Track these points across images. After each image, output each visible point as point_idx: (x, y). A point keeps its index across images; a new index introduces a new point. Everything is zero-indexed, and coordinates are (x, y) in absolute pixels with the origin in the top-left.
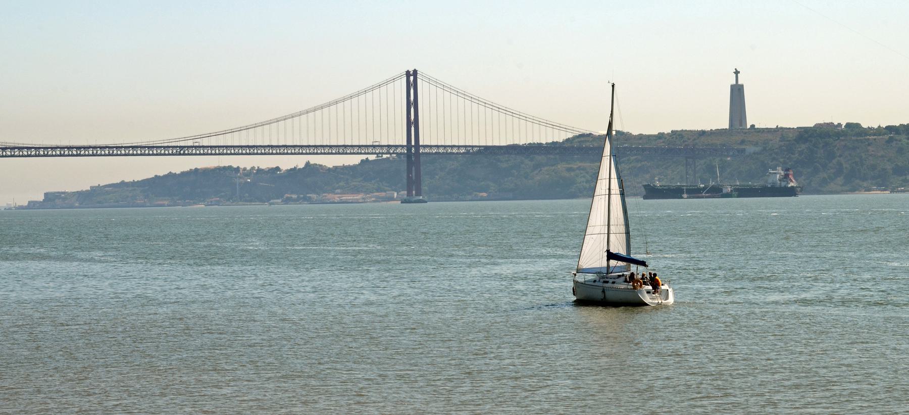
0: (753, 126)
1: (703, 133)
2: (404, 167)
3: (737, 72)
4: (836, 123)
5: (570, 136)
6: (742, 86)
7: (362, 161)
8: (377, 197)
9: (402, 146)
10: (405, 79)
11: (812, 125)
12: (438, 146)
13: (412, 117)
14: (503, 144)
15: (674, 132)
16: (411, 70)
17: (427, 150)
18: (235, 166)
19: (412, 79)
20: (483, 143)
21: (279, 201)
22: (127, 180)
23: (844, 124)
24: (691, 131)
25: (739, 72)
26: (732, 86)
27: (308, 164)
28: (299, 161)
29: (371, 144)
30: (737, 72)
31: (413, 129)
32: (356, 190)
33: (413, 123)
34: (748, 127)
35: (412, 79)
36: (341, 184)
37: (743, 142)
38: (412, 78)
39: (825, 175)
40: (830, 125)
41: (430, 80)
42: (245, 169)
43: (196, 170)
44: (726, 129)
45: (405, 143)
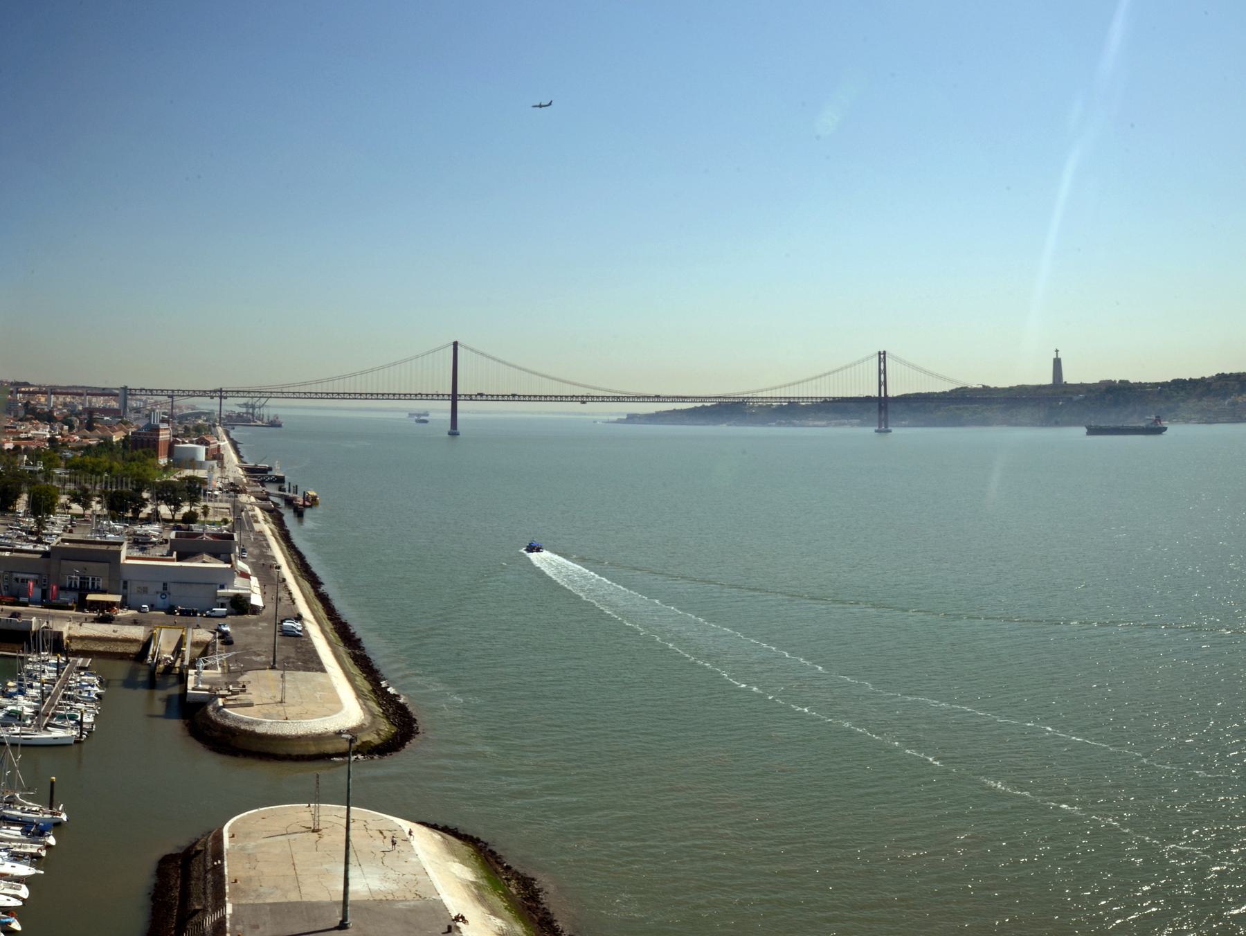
3: (1057, 351)
11: (1098, 381)
13: (882, 380)
30: (1057, 351)
31: (883, 387)
33: (883, 384)
37: (1065, 392)
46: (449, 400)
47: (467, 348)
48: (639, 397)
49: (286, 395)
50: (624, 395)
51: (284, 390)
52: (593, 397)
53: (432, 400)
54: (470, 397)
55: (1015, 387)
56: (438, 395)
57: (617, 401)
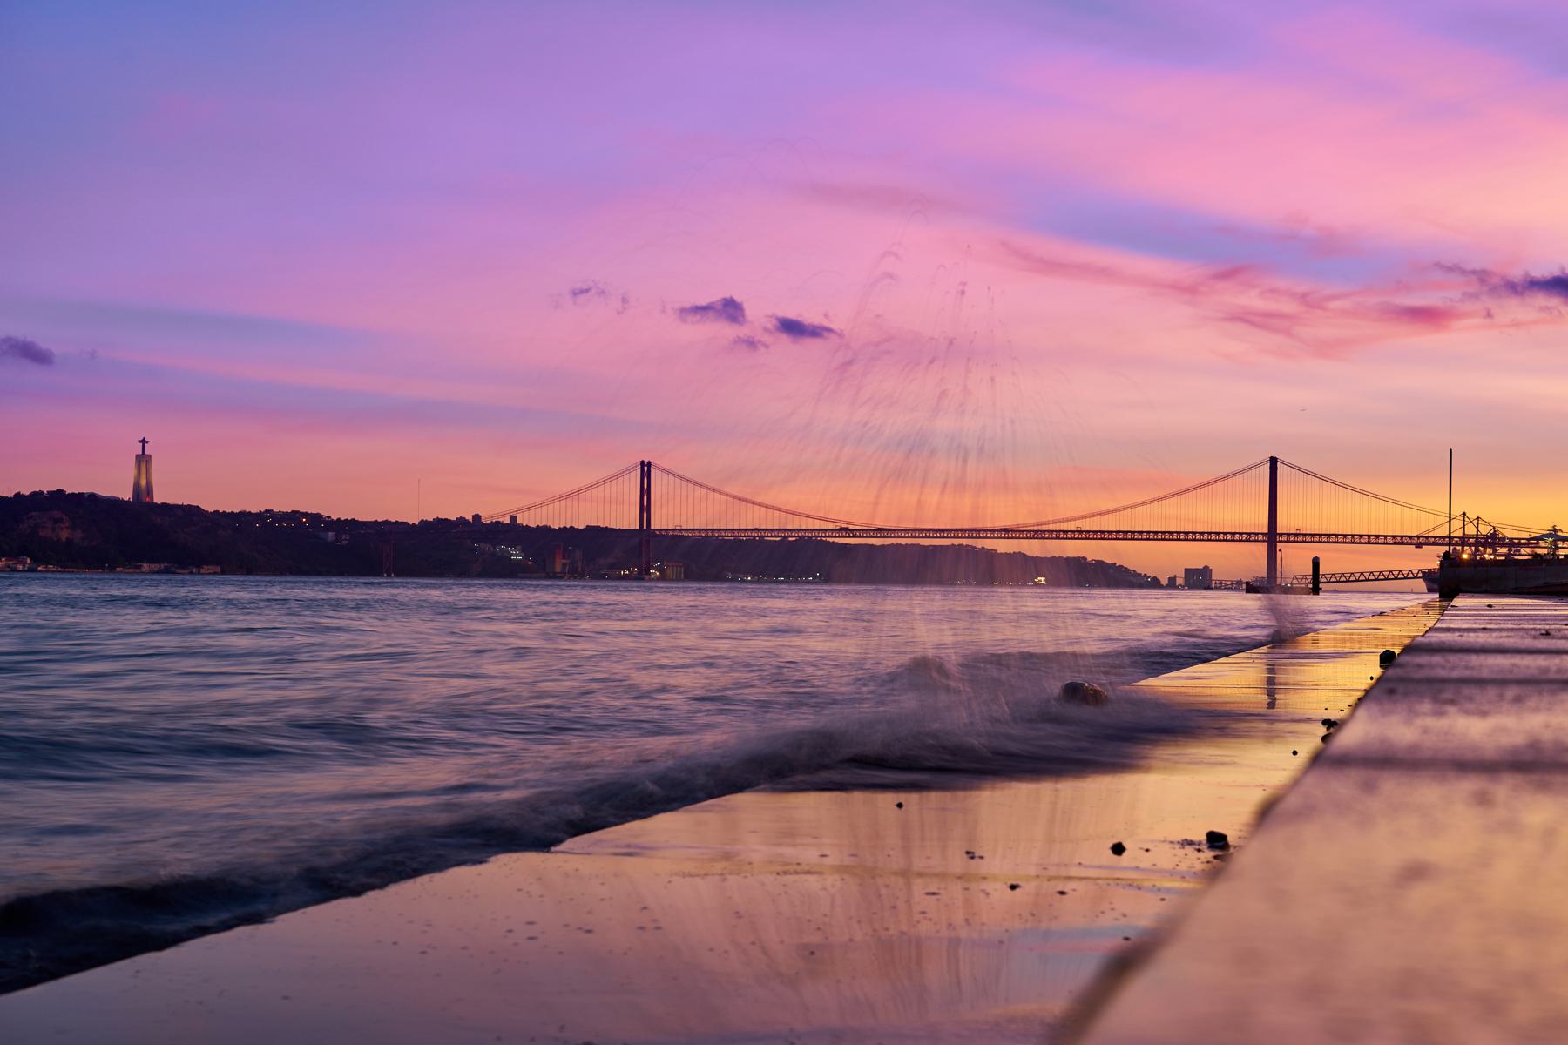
16: (646, 460)
19: (646, 469)
25: (144, 438)
33: (645, 509)
35: (646, 469)
38: (646, 468)
44: (114, 503)
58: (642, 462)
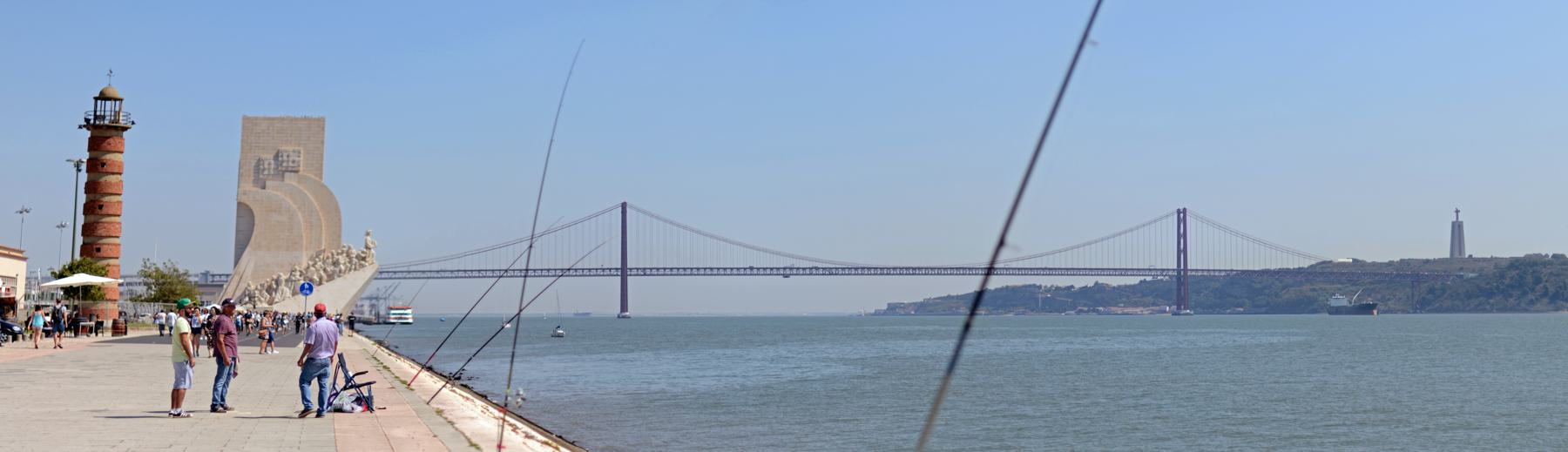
0: (1470, 256)
1: (1427, 261)
2: (1174, 286)
3: (1457, 211)
4: (1544, 254)
5: (1314, 262)
6: (1462, 222)
7: (1141, 282)
8: (1153, 310)
9: (1174, 270)
10: (1176, 216)
11: (1522, 256)
12: (1203, 270)
14: (1257, 269)
15: (1402, 261)
16: (1181, 208)
17: (1193, 273)
18: (1038, 284)
19: (1182, 216)
20: (1240, 268)
21: (1073, 312)
22: (952, 294)
23: (1551, 255)
24: (1416, 260)
26: (1453, 223)
27: (1096, 283)
28: (1089, 281)
29: (1148, 267)
30: (1457, 211)
32: (1136, 305)
33: (1182, 252)
34: (1467, 256)
35: (1182, 216)
36: (1124, 299)
37: (1461, 269)
38: (1182, 215)
39: (1533, 298)
40: (1538, 255)
41: (1197, 217)
42: (1046, 287)
43: (1007, 287)
45: (1175, 267)
46: (617, 275)
47: (638, 210)
48: (856, 269)
49: (429, 275)
50: (837, 266)
51: (412, 269)
52: (798, 269)
53: (664, 275)
54: (644, 272)
55: (1361, 261)
56: (603, 270)
57: (830, 274)
58: (1179, 210)
